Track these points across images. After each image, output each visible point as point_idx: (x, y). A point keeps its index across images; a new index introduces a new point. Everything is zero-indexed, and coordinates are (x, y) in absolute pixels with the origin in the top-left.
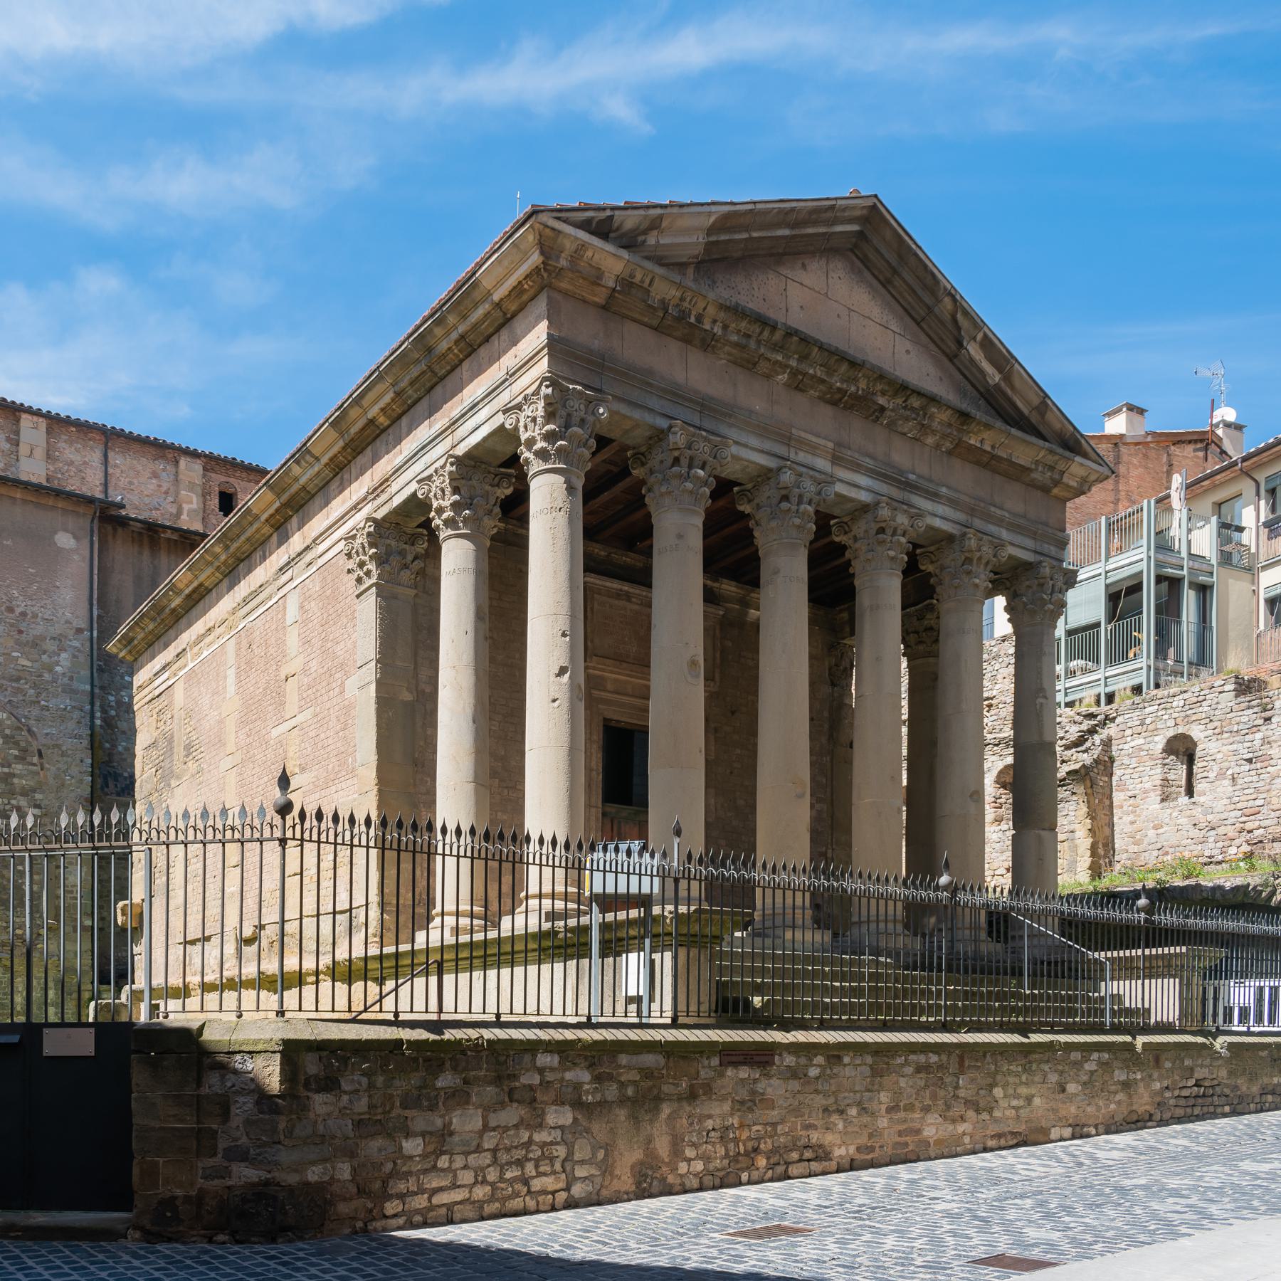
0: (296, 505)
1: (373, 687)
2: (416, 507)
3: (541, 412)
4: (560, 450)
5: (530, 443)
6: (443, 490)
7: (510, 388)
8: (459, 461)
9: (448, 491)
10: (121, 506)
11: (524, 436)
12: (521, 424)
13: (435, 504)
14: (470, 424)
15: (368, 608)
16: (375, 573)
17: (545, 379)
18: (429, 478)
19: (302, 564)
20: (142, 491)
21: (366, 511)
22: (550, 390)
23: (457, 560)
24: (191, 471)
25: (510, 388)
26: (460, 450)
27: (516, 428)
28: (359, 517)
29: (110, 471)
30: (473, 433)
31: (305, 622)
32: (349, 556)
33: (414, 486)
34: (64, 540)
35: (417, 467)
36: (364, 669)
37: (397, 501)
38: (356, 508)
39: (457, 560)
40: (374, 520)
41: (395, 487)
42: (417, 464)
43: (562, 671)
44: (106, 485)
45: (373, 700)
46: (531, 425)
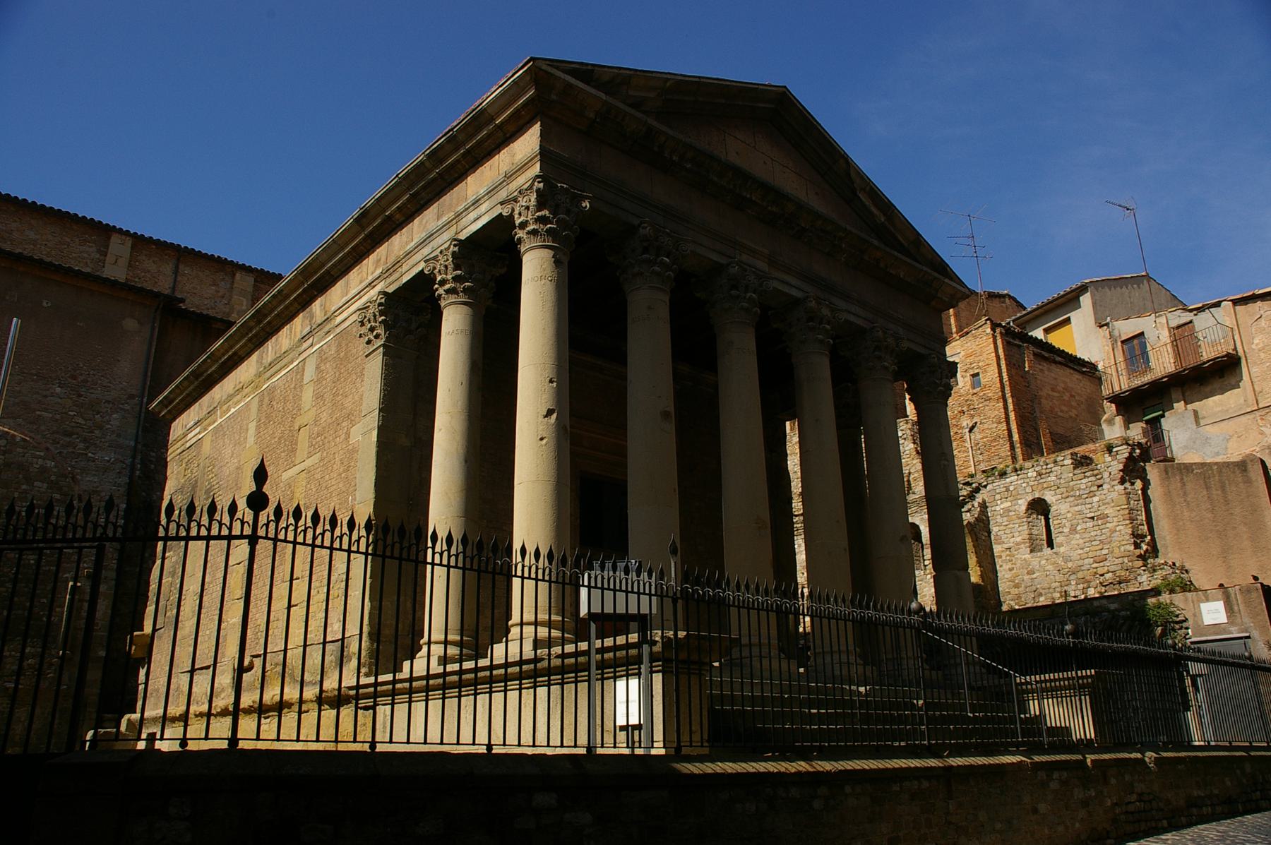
0: (317, 279)
1: (375, 433)
2: (423, 282)
3: (533, 202)
4: (549, 231)
5: (523, 225)
6: (446, 267)
7: (507, 178)
8: (460, 243)
9: (451, 267)
10: (182, 301)
11: (517, 223)
12: (516, 212)
13: (439, 278)
14: (472, 215)
15: (375, 367)
16: (383, 336)
17: (537, 177)
18: (435, 258)
19: (321, 333)
20: (199, 294)
21: (378, 288)
22: (541, 185)
23: (454, 324)
24: (244, 282)
25: (507, 178)
26: (463, 236)
27: (511, 216)
28: (373, 293)
29: (179, 278)
30: (473, 224)
31: (319, 380)
32: (362, 324)
33: (422, 265)
34: (130, 324)
35: (426, 251)
36: (368, 418)
37: (405, 279)
38: (371, 285)
39: (454, 324)
40: (385, 293)
41: (405, 268)
42: (423, 243)
43: (549, 413)
44: (174, 289)
45: (375, 444)
46: (524, 212)
